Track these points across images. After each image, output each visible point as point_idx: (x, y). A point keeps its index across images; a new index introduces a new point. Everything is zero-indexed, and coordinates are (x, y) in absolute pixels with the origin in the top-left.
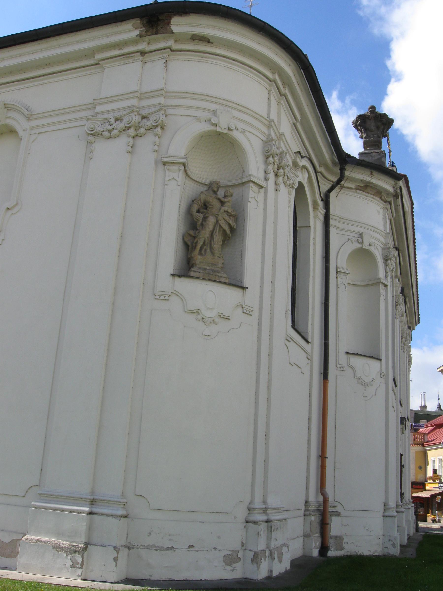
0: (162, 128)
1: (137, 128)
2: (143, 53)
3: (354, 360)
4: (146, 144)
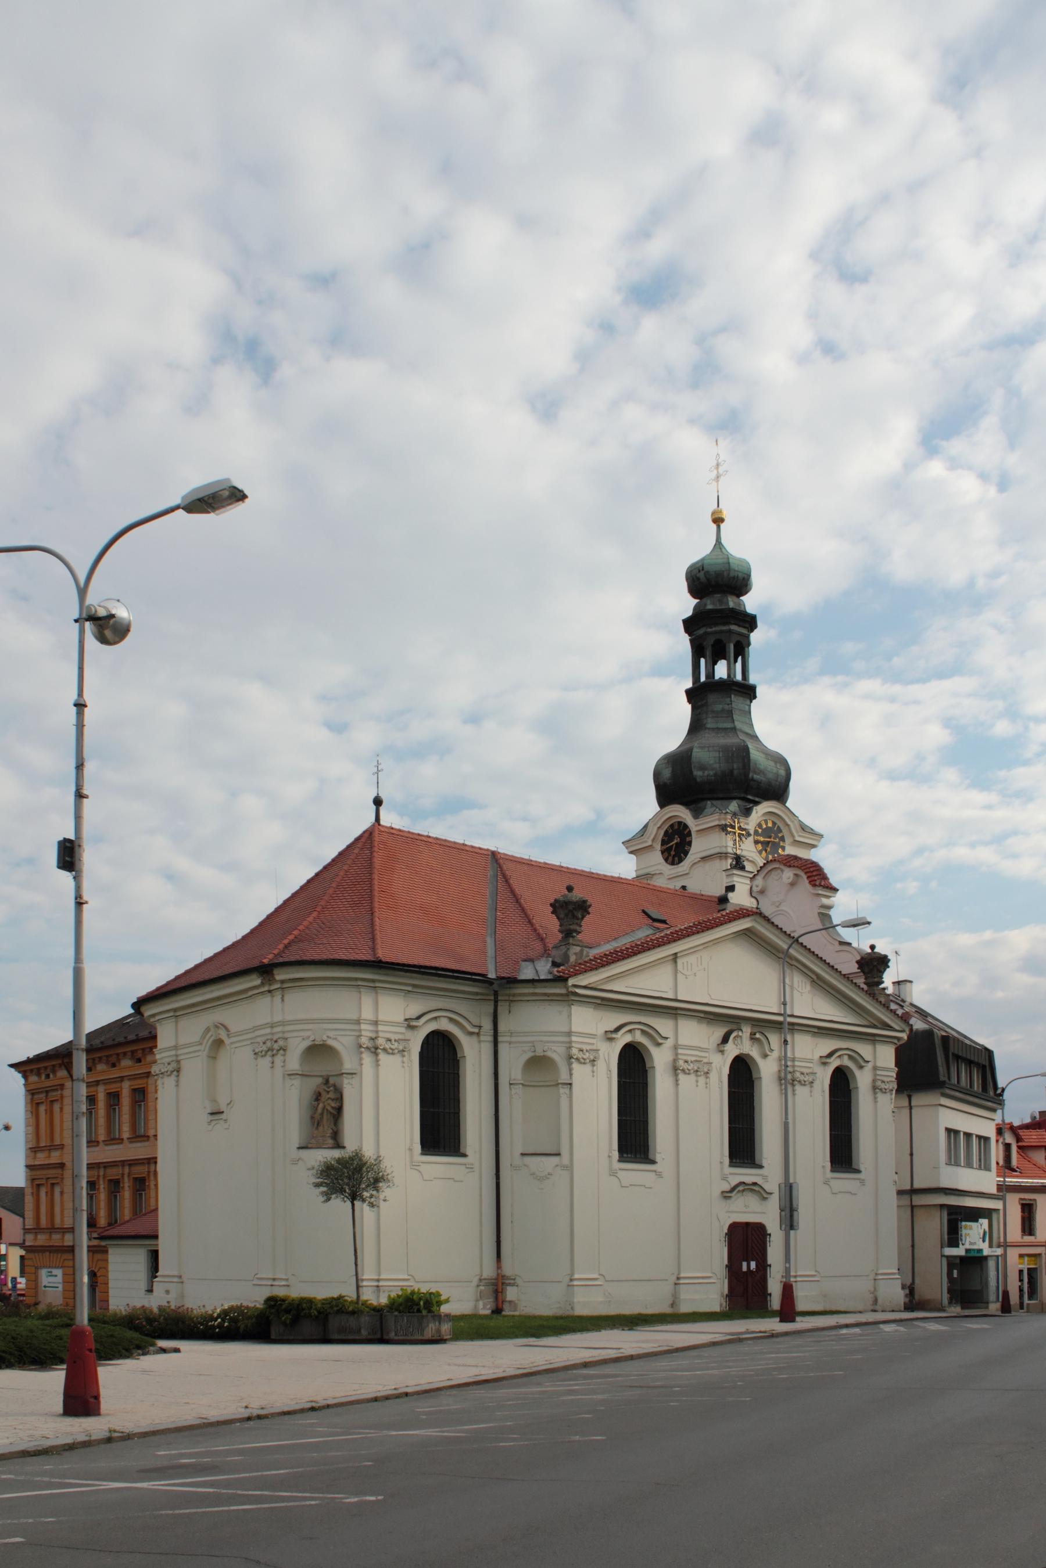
0: (284, 1050)
1: (273, 1050)
2: (269, 991)
3: (527, 1159)
4: (279, 1059)
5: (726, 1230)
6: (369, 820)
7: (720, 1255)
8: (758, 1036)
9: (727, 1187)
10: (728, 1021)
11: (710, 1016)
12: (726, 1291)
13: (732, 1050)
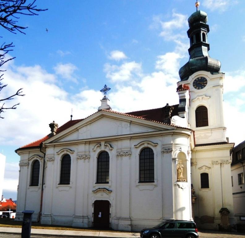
5: (93, 202)
6: (70, 120)
7: (92, 210)
8: (106, 144)
9: (94, 189)
10: (97, 142)
11: (88, 142)
12: (93, 221)
13: (99, 150)
